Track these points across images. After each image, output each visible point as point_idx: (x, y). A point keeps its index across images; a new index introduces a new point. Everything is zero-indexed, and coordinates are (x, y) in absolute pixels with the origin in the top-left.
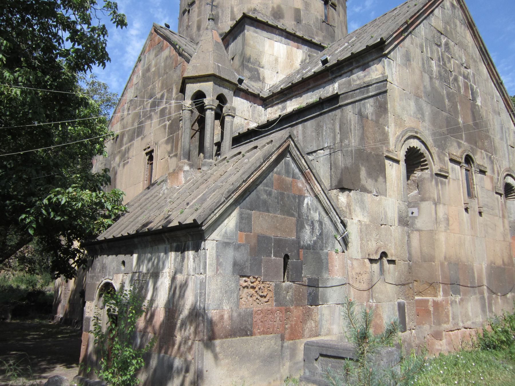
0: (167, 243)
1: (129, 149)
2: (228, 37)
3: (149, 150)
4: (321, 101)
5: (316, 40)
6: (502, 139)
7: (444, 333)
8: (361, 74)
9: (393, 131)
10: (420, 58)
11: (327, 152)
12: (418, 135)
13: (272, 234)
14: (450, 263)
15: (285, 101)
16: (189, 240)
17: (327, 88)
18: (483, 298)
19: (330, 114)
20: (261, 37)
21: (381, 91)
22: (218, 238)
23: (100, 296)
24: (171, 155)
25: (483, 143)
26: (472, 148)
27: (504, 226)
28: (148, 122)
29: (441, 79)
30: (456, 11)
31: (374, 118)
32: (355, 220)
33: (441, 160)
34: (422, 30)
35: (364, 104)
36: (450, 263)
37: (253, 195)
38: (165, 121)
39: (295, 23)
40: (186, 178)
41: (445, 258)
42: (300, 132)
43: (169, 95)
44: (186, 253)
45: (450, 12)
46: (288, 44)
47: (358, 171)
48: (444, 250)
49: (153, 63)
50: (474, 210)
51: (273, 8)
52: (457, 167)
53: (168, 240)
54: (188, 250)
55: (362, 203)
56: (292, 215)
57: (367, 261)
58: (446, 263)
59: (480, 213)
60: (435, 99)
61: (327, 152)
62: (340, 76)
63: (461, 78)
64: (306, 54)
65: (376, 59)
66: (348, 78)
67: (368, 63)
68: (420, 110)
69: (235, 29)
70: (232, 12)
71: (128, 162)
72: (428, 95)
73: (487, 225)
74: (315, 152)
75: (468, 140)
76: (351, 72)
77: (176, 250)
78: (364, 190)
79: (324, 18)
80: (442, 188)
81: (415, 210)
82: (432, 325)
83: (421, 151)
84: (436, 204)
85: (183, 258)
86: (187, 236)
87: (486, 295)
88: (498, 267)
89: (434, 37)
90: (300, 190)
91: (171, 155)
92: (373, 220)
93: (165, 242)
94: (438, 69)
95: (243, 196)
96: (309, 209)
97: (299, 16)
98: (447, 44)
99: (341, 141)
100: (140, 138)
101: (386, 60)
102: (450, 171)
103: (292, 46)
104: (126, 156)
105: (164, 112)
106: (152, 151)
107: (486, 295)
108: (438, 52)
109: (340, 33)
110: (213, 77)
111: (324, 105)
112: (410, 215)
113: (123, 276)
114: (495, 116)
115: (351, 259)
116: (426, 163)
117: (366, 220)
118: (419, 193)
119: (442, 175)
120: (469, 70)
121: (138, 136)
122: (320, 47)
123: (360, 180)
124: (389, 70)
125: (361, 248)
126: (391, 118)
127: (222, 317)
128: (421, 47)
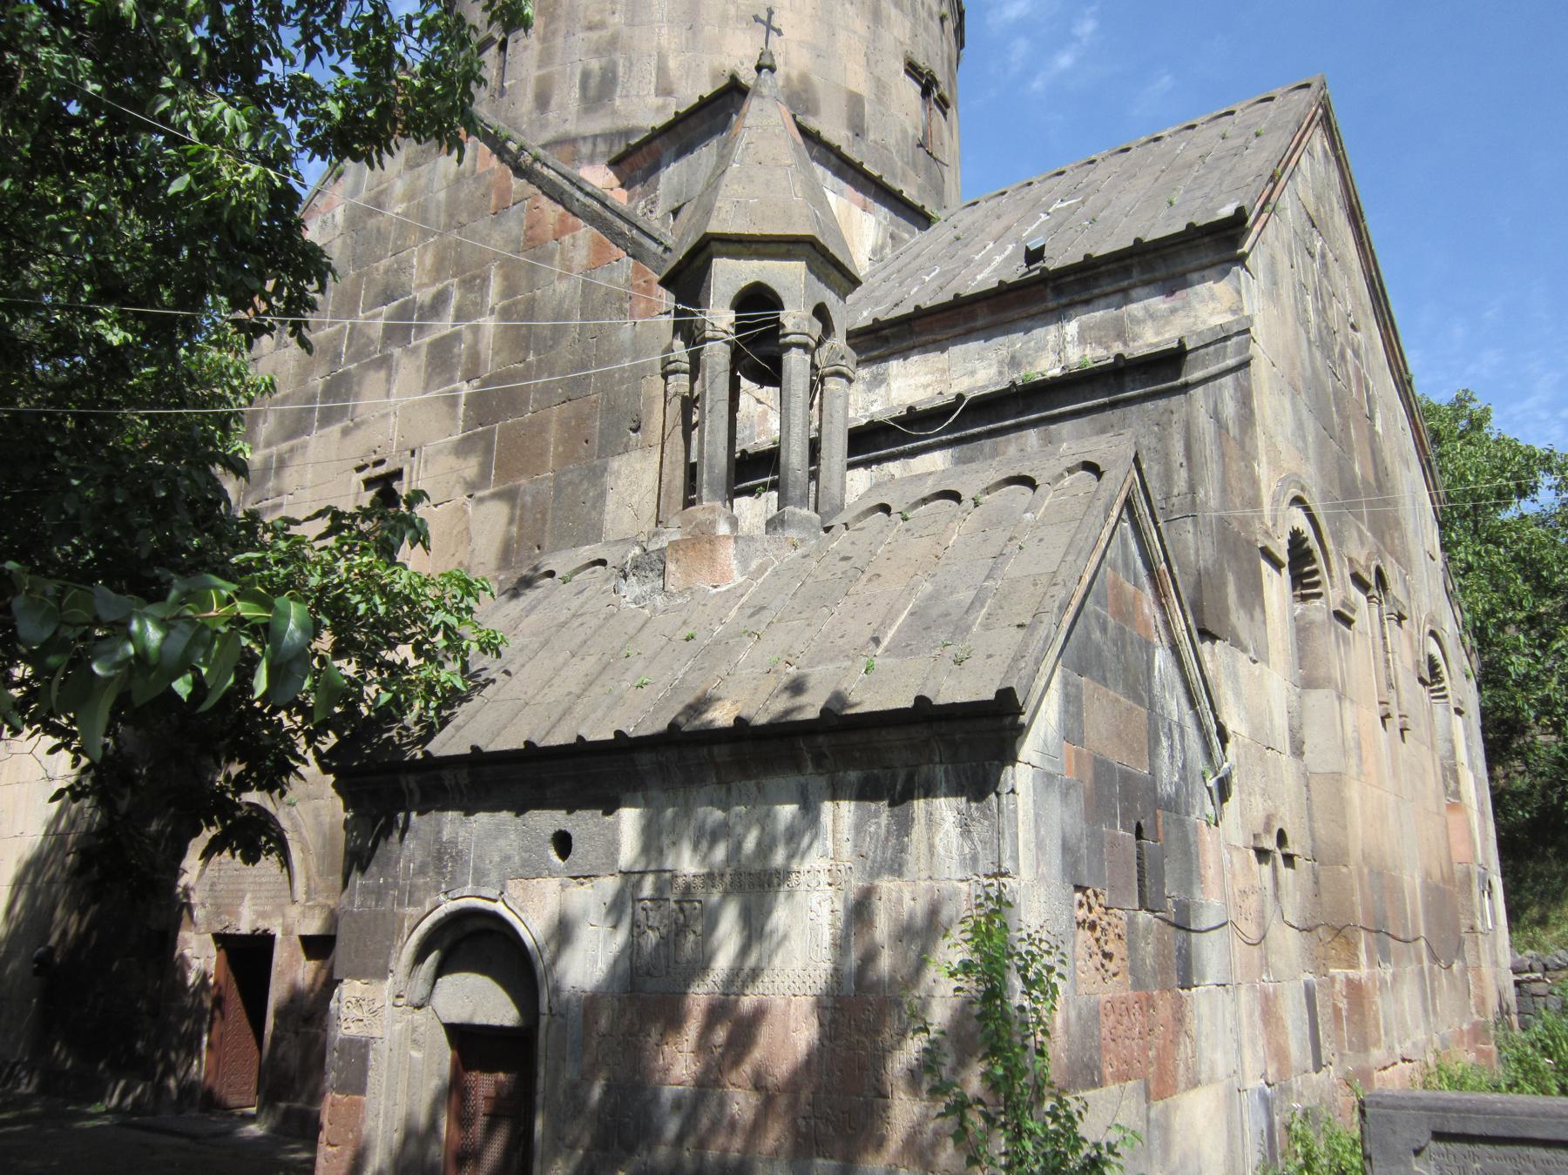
0: (810, 769)
1: (282, 464)
2: (657, 143)
4: (1122, 364)
7: (1376, 1074)
8: (1159, 303)
15: (884, 359)
16: (931, 761)
17: (1038, 333)
19: (1149, 405)
23: (419, 958)
24: (479, 494)
28: (376, 378)
38: (451, 380)
39: (850, 135)
40: (744, 561)
43: (472, 296)
44: (919, 805)
49: (399, 187)
53: (819, 760)
54: (929, 792)
57: (1252, 853)
58: (1366, 870)
62: (1087, 302)
63: (1349, 353)
64: (885, 229)
65: (1213, 265)
66: (1112, 312)
67: (1183, 274)
69: (693, 122)
70: (662, 70)
76: (1125, 296)
77: (865, 793)
79: (920, 135)
82: (1346, 1051)
84: (1339, 698)
85: (903, 826)
91: (479, 494)
93: (798, 767)
97: (861, 116)
100: (336, 429)
103: (852, 200)
104: (270, 484)
105: (450, 350)
110: (808, 247)
111: (1127, 379)
113: (563, 886)
115: (1229, 846)
116: (1316, 578)
121: (327, 418)
125: (1242, 815)
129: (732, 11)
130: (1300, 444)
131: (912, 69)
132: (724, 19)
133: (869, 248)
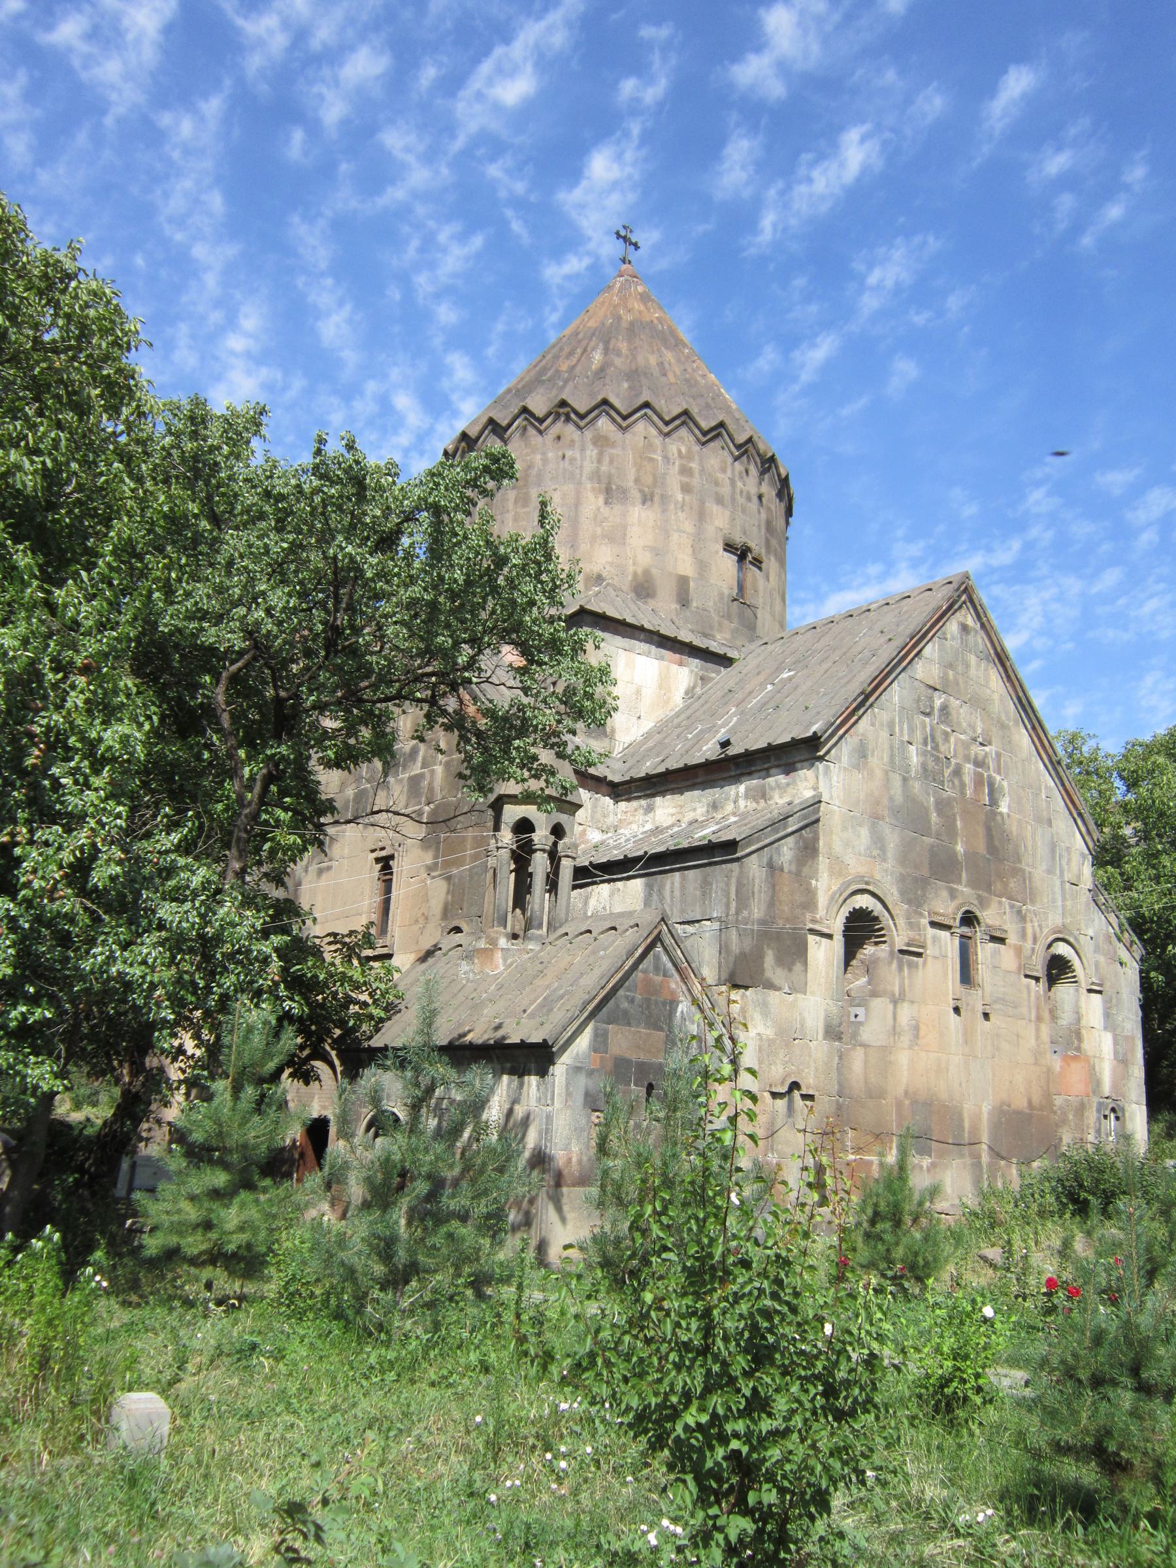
3: (384, 853)
5: (714, 647)
6: (1050, 871)
8: (782, 779)
9: (825, 885)
10: (886, 746)
11: (716, 925)
12: (870, 888)
13: (634, 1058)
14: (914, 1102)
15: (653, 795)
18: (977, 1165)
20: (612, 648)
21: (809, 819)
22: (569, 1061)
23: (368, 1130)
25: (1006, 885)
26: (979, 898)
27: (1038, 1038)
29: (926, 778)
30: (971, 638)
31: (793, 868)
32: (753, 1032)
33: (911, 926)
34: (897, 694)
35: (778, 849)
36: (914, 1102)
37: (612, 1003)
40: (505, 960)
41: (906, 1093)
42: (677, 885)
45: (956, 644)
46: (662, 658)
47: (760, 957)
48: (904, 1081)
50: (973, 1010)
51: (635, 574)
52: (944, 935)
55: (764, 1006)
56: (661, 1029)
57: (767, 1095)
58: (907, 1102)
59: (986, 1016)
60: (911, 817)
61: (716, 925)
62: (750, 774)
63: (969, 768)
68: (878, 841)
71: (329, 868)
72: (895, 812)
73: (998, 1036)
74: (698, 921)
75: (973, 883)
77: (511, 1073)
78: (770, 986)
80: (910, 973)
81: (860, 1011)
83: (875, 914)
84: (895, 1002)
85: (521, 1085)
86: (532, 1058)
87: (985, 1158)
88: (1018, 1113)
89: (918, 700)
90: (673, 993)
92: (781, 1032)
94: (921, 759)
95: (602, 1008)
96: (683, 1019)
98: (944, 708)
99: (737, 913)
101: (821, 766)
102: (929, 942)
106: (392, 857)
107: (985, 1158)
108: (924, 727)
109: (768, 616)
112: (852, 1019)
114: (1040, 830)
117: (769, 1033)
118: (869, 983)
119: (911, 953)
120: (987, 749)
122: (724, 661)
123: (763, 971)
124: (827, 784)
126: (823, 862)
127: (569, 1160)
128: (891, 725)
129: (599, 531)
130: (875, 853)
131: (729, 547)
132: (594, 538)
133: (682, 691)
